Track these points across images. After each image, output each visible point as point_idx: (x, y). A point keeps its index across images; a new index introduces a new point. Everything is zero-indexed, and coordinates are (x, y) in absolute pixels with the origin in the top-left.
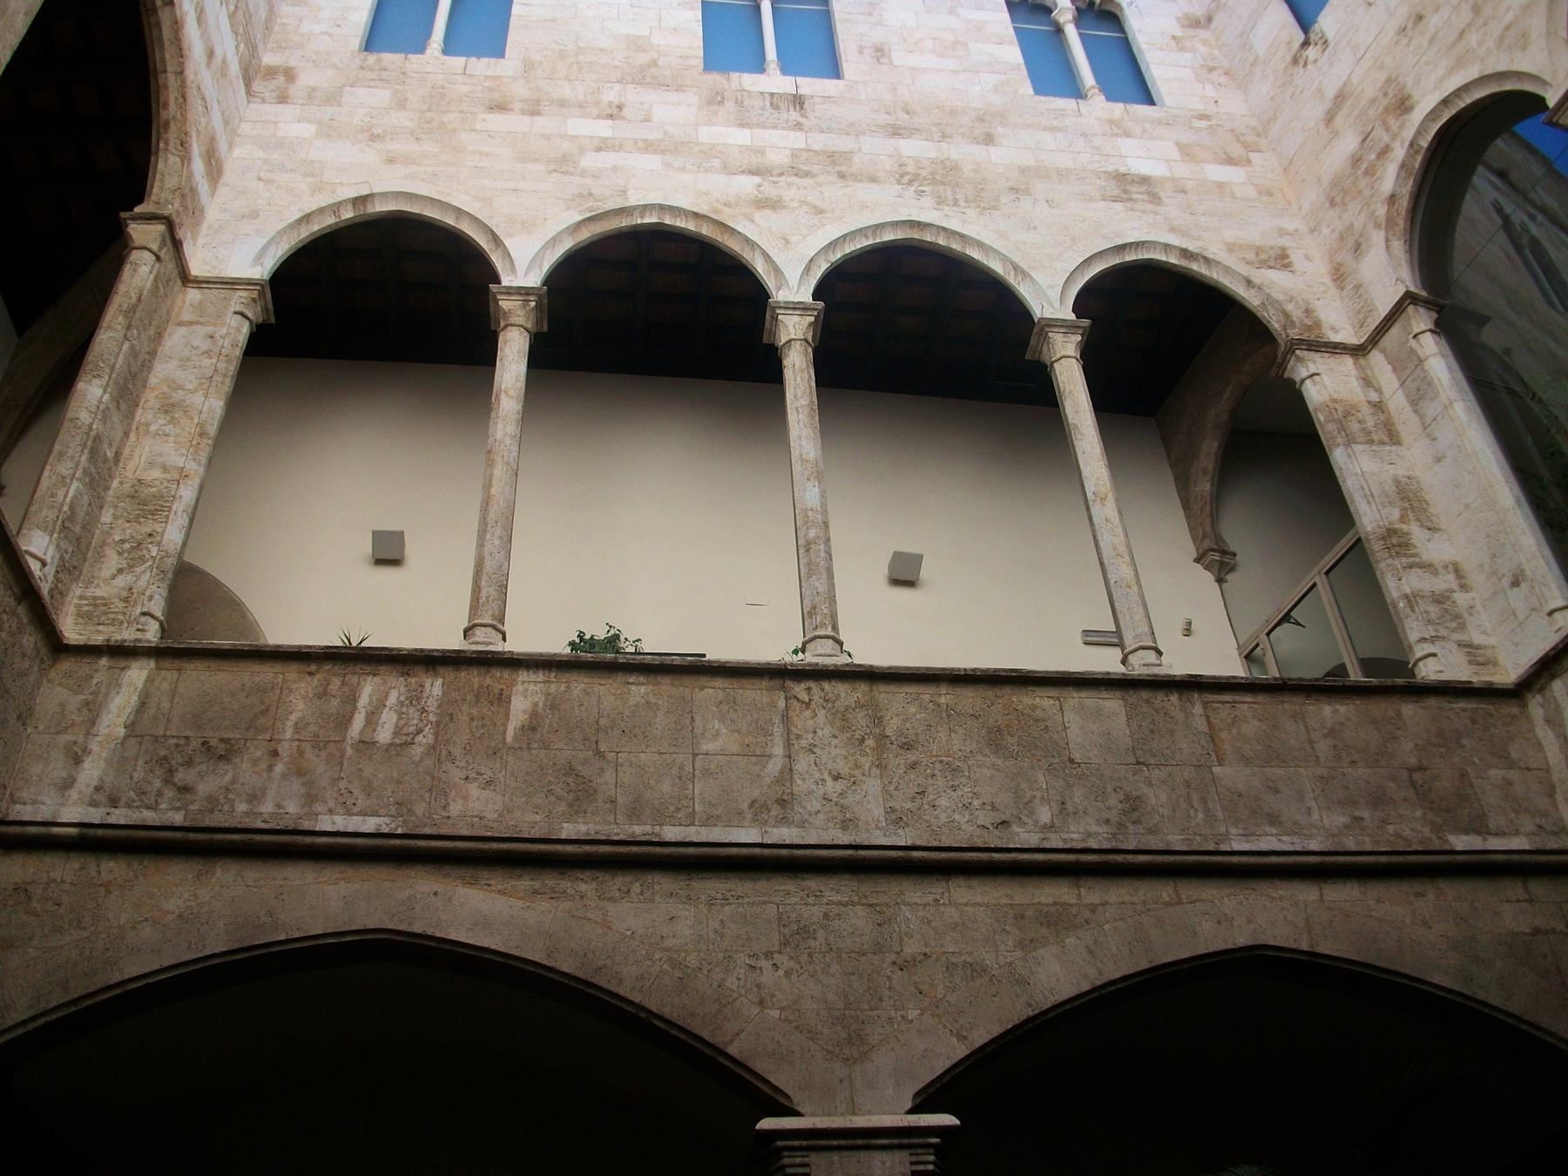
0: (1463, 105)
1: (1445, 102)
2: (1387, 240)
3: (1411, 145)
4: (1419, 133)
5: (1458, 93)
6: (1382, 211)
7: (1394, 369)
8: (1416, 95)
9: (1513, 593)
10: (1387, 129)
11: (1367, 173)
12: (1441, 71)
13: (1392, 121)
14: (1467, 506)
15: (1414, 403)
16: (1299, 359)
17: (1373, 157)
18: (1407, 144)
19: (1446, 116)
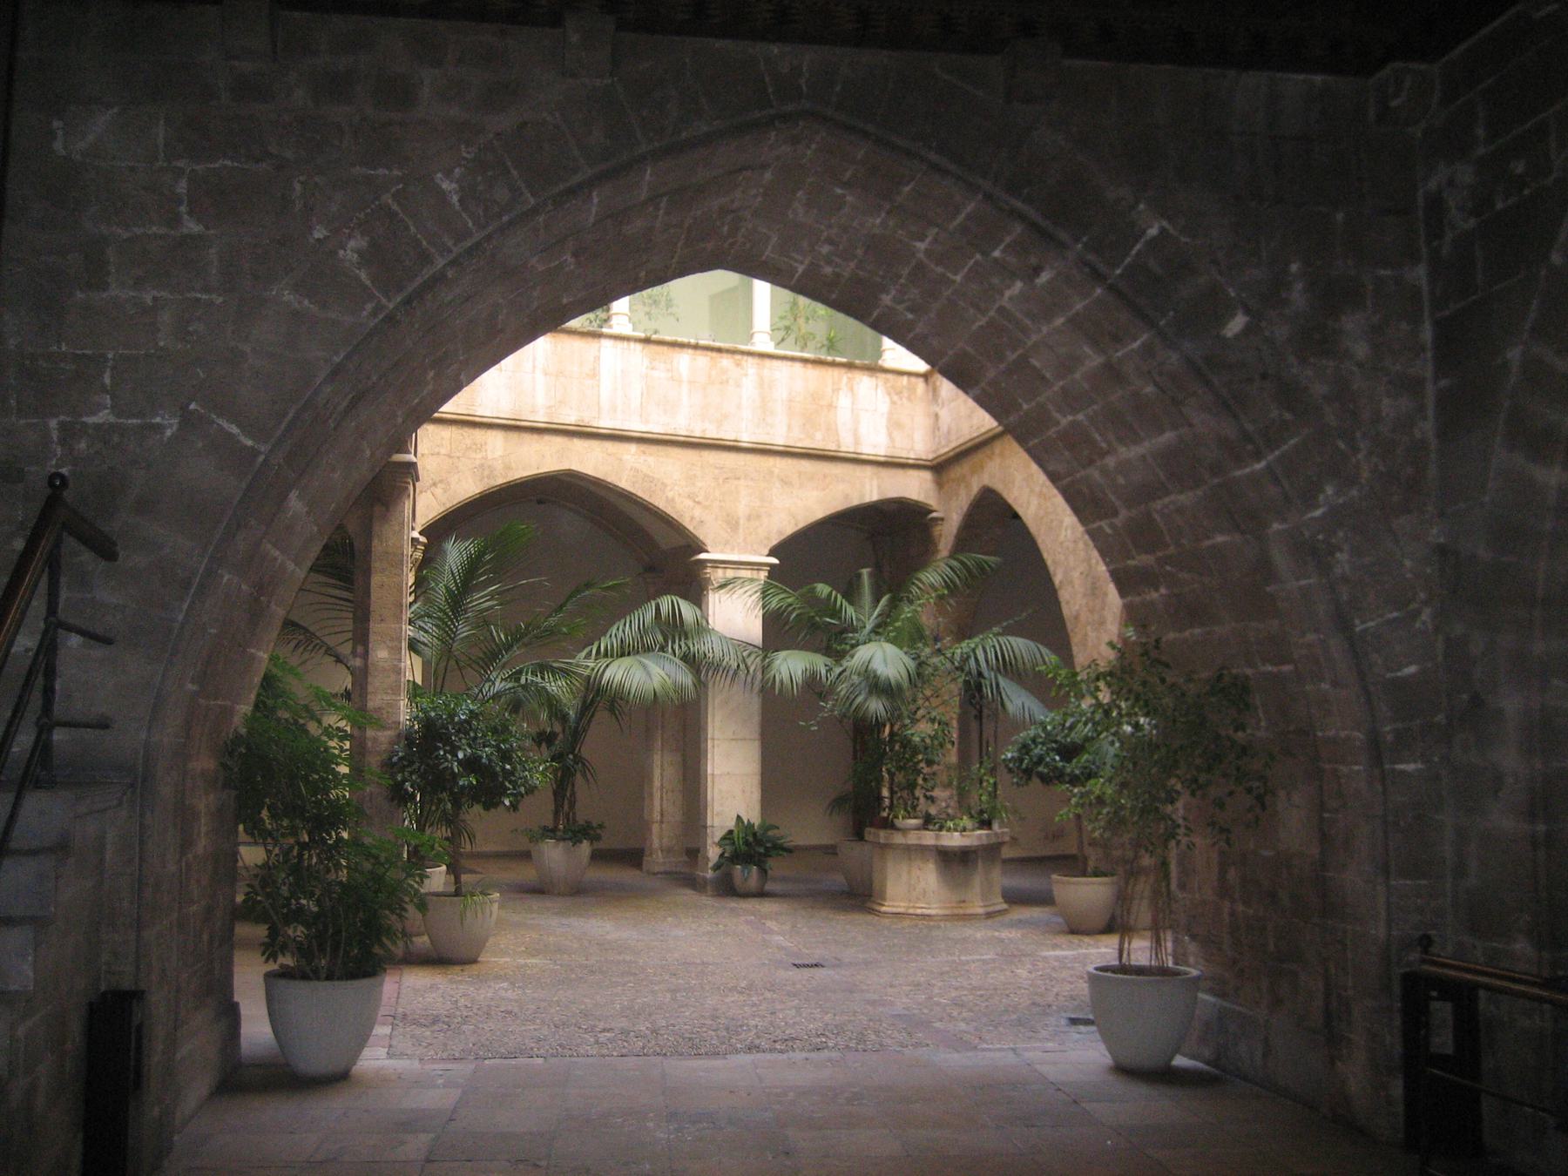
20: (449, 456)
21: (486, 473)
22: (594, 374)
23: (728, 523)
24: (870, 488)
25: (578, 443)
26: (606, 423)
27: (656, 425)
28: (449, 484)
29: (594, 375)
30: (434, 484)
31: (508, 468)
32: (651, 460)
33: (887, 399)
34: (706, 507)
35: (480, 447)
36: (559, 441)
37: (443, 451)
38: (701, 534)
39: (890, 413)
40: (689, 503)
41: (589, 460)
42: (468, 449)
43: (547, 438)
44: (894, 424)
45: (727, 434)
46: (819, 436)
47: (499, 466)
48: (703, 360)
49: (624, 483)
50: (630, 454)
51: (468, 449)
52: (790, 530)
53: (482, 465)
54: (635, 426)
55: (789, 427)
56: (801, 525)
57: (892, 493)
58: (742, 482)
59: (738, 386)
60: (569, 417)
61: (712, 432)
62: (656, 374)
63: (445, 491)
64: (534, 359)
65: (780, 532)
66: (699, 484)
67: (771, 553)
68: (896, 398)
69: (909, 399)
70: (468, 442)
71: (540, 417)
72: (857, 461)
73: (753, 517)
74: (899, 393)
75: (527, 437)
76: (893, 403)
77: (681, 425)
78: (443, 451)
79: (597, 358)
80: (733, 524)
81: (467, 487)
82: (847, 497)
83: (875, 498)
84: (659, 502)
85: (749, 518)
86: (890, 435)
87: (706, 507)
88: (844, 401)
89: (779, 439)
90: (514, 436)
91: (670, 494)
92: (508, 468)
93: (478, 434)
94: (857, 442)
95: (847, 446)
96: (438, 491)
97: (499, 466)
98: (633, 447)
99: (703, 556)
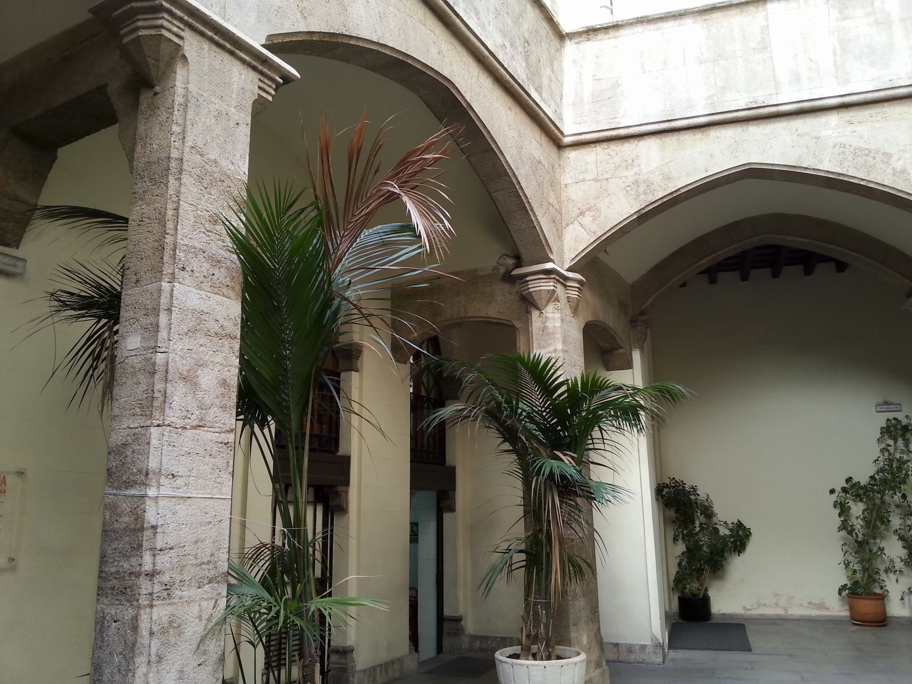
20: (596, 180)
21: (641, 189)
22: (764, 46)
25: (754, 130)
26: (788, 95)
27: (863, 81)
28: (598, 210)
29: (764, 48)
30: (582, 214)
32: (861, 129)
35: (631, 163)
37: (588, 176)
42: (618, 167)
43: (714, 133)
47: (657, 179)
51: (618, 167)
53: (636, 182)
54: (829, 89)
70: (617, 159)
71: (700, 110)
75: (686, 137)
78: (588, 176)
79: (765, 29)
81: (620, 208)
90: (671, 140)
91: (898, 165)
92: (668, 178)
93: (627, 148)
96: (587, 220)
98: (833, 119)
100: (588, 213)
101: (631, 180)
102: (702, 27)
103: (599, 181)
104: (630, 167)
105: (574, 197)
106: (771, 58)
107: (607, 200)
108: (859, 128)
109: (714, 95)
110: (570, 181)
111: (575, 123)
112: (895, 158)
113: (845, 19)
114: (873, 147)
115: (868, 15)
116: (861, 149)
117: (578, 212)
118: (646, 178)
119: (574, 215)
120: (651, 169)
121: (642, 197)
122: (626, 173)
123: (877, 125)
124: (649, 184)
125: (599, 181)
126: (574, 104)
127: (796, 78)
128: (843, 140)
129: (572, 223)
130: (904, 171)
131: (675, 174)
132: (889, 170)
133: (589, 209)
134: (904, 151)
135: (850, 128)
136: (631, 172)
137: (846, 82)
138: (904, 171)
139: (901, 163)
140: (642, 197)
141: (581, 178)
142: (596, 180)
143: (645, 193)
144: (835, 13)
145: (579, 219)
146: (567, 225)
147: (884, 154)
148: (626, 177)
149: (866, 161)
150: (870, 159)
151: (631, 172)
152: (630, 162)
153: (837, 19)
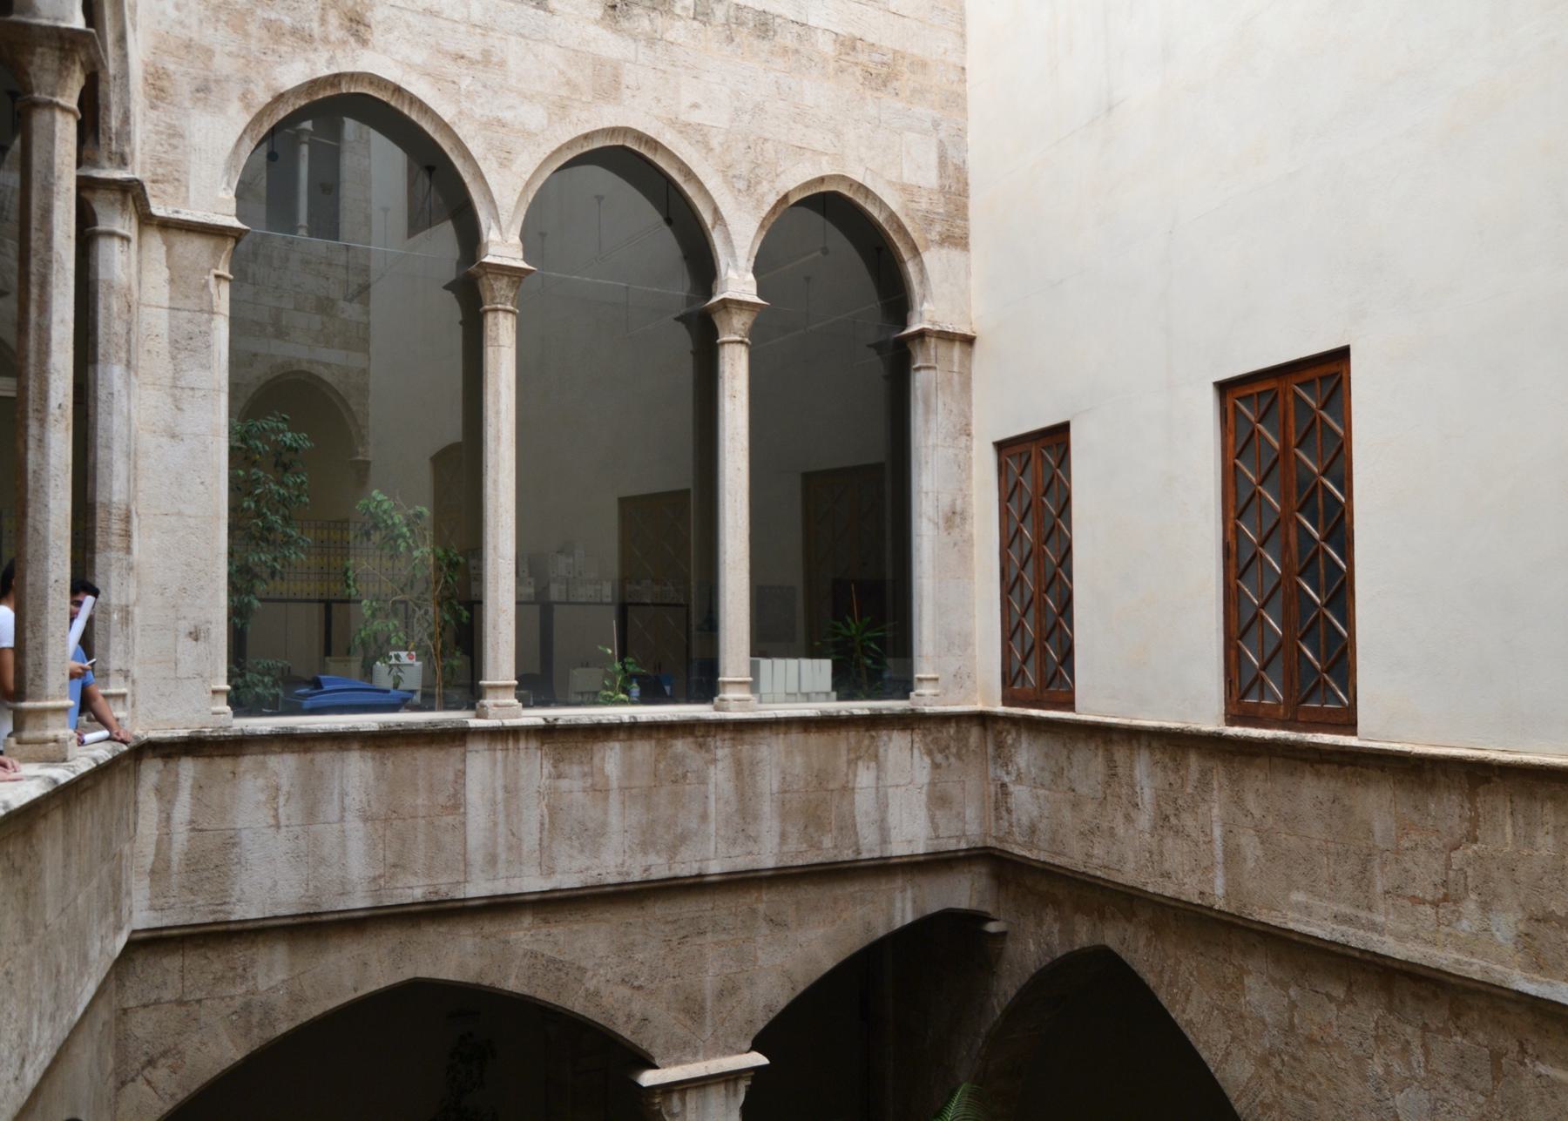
0: (406, 111)
1: (398, 90)
2: (245, 131)
3: (336, 76)
4: (354, 77)
5: (414, 101)
6: (263, 98)
7: (172, 281)
8: (377, 37)
9: (186, 644)
10: (323, 21)
11: (268, 25)
12: (419, 57)
13: (333, 19)
14: (180, 514)
15: (174, 343)
16: (124, 204)
17: (288, 21)
18: (335, 70)
19: (383, 96)
20: (181, 1002)
21: (255, 1019)
22: (456, 804)
23: (687, 1011)
24: (902, 907)
25: (431, 934)
26: (478, 888)
29: (456, 807)
30: (151, 1062)
31: (297, 999)
33: (927, 760)
34: (652, 993)
36: (391, 938)
37: (168, 995)
38: (643, 1041)
39: (932, 784)
40: (623, 991)
41: (453, 958)
44: (939, 800)
45: (685, 867)
46: (828, 842)
47: (281, 999)
48: (643, 749)
49: (513, 983)
50: (524, 935)
52: (782, 1002)
53: (247, 1007)
54: (532, 882)
55: (783, 836)
56: (801, 988)
57: (933, 907)
58: (709, 935)
59: (703, 781)
60: (413, 890)
61: (660, 868)
62: (564, 784)
63: (174, 1070)
64: (343, 795)
65: (769, 1008)
66: (640, 956)
67: (757, 1046)
68: (939, 758)
69: (959, 756)
71: (359, 901)
72: (885, 868)
73: (727, 990)
74: (944, 750)
76: (936, 766)
77: (614, 863)
80: (693, 1009)
82: (868, 926)
83: (909, 919)
84: (576, 1003)
85: (720, 995)
86: (932, 818)
87: (652, 993)
88: (865, 778)
89: (767, 857)
91: (591, 985)
94: (885, 840)
95: (870, 847)
96: (160, 1074)
97: (281, 999)
99: (648, 1078)
100: (163, 1061)
101: (238, 1002)
102: (373, 759)
103: (186, 1003)
104: (238, 980)
105: (139, 1032)
106: (464, 824)
107: (196, 1038)
108: (554, 931)
109: (380, 876)
110: (132, 1003)
111: (152, 908)
112: (590, 974)
113: (559, 777)
114: (567, 958)
115: (585, 775)
116: (553, 961)
117: (144, 1059)
118: (264, 999)
119: (137, 1065)
120: (272, 983)
121: (256, 1031)
122: (233, 991)
123: (576, 927)
124: (268, 1010)
125: (186, 1003)
126: (152, 872)
127: (492, 860)
128: (535, 947)
129: (133, 1080)
130: (597, 993)
131: (309, 993)
132: (582, 993)
133: (164, 1054)
134: (600, 965)
135: (544, 931)
136: (241, 990)
137: (551, 872)
138: (597, 993)
139: (594, 981)
140: (256, 1031)
141: (153, 997)
142: (181, 1002)
143: (261, 1025)
144: (548, 767)
145: (146, 1072)
146: (123, 1084)
147: (579, 968)
148: (232, 998)
149: (559, 978)
150: (562, 975)
151: (241, 990)
152: (240, 970)
153: (550, 776)
